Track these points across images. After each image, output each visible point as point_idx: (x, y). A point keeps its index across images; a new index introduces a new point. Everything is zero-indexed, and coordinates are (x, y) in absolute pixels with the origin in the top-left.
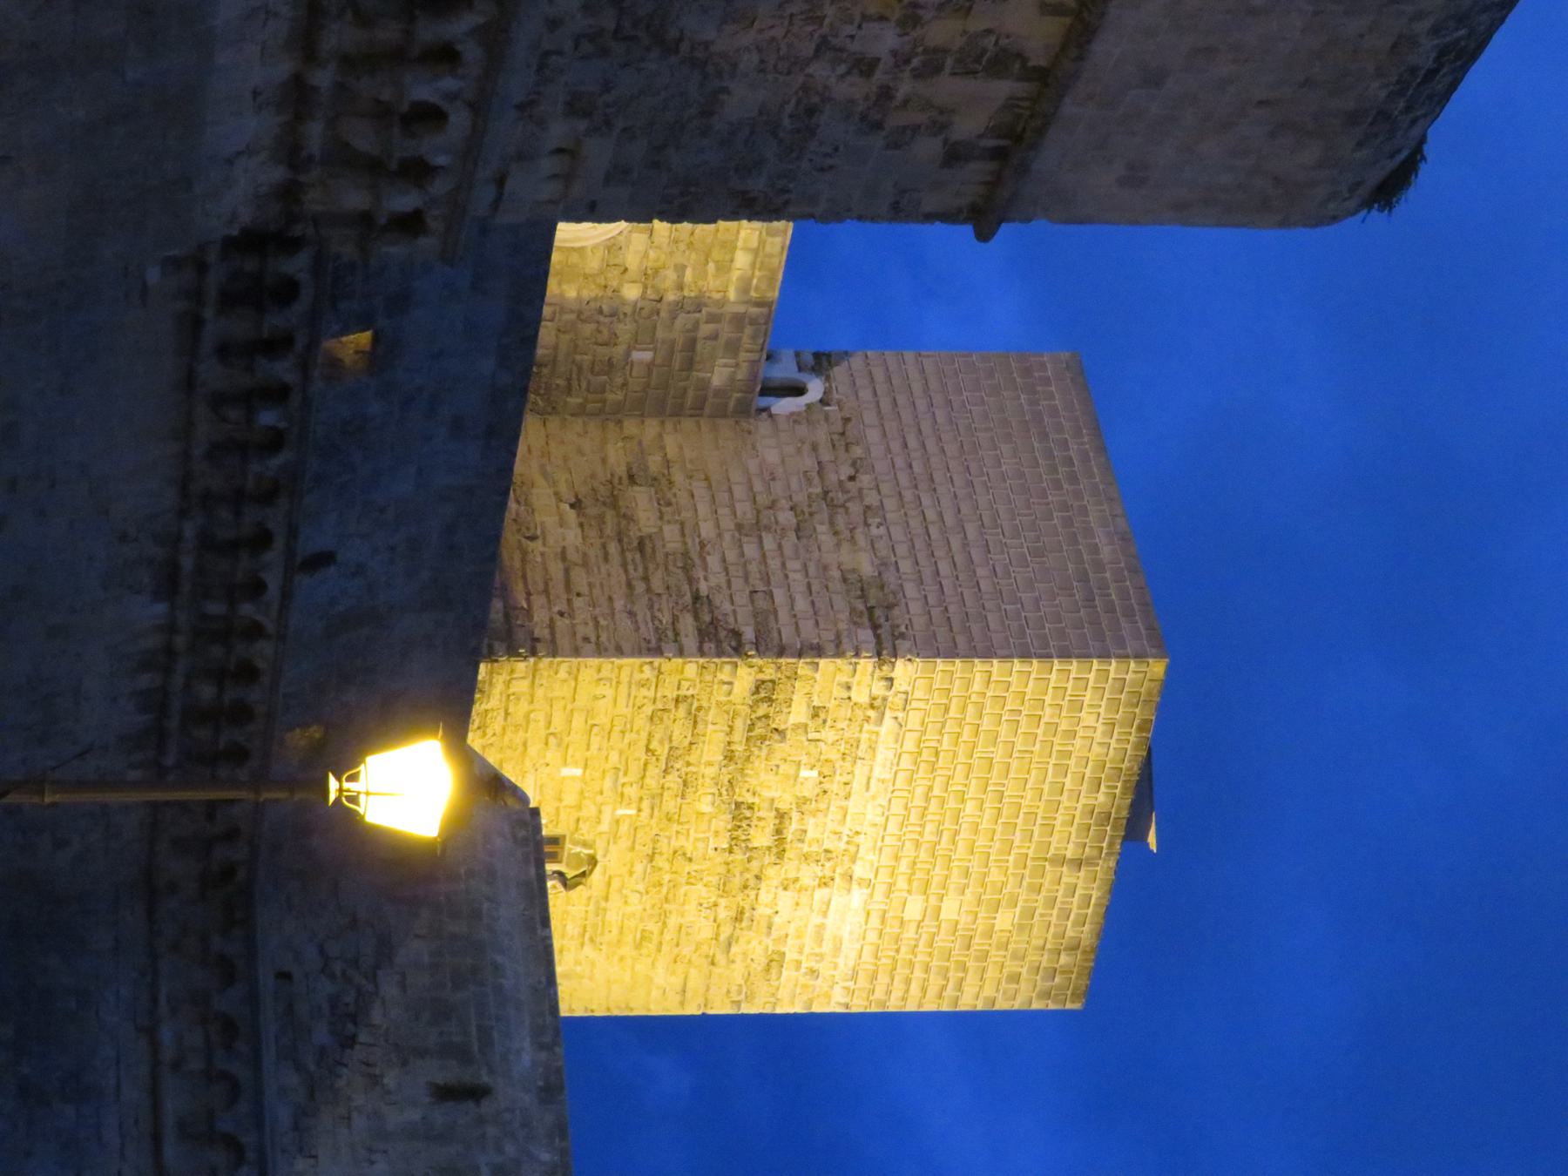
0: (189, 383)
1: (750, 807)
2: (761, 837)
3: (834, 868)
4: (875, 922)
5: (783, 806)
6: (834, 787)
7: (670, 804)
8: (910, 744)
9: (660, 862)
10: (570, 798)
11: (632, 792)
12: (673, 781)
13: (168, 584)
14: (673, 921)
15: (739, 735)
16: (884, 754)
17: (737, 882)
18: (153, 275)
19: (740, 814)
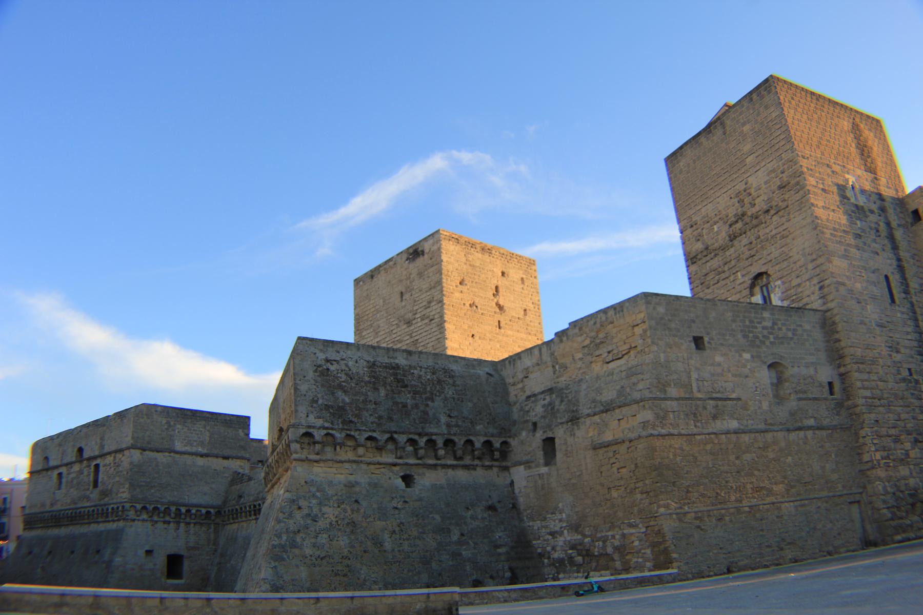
1: (730, 237)
2: (739, 225)
5: (728, 227)
6: (716, 219)
9: (753, 253)
11: (732, 278)
12: (726, 268)
14: (774, 232)
15: (708, 258)
17: (755, 222)
19: (733, 238)
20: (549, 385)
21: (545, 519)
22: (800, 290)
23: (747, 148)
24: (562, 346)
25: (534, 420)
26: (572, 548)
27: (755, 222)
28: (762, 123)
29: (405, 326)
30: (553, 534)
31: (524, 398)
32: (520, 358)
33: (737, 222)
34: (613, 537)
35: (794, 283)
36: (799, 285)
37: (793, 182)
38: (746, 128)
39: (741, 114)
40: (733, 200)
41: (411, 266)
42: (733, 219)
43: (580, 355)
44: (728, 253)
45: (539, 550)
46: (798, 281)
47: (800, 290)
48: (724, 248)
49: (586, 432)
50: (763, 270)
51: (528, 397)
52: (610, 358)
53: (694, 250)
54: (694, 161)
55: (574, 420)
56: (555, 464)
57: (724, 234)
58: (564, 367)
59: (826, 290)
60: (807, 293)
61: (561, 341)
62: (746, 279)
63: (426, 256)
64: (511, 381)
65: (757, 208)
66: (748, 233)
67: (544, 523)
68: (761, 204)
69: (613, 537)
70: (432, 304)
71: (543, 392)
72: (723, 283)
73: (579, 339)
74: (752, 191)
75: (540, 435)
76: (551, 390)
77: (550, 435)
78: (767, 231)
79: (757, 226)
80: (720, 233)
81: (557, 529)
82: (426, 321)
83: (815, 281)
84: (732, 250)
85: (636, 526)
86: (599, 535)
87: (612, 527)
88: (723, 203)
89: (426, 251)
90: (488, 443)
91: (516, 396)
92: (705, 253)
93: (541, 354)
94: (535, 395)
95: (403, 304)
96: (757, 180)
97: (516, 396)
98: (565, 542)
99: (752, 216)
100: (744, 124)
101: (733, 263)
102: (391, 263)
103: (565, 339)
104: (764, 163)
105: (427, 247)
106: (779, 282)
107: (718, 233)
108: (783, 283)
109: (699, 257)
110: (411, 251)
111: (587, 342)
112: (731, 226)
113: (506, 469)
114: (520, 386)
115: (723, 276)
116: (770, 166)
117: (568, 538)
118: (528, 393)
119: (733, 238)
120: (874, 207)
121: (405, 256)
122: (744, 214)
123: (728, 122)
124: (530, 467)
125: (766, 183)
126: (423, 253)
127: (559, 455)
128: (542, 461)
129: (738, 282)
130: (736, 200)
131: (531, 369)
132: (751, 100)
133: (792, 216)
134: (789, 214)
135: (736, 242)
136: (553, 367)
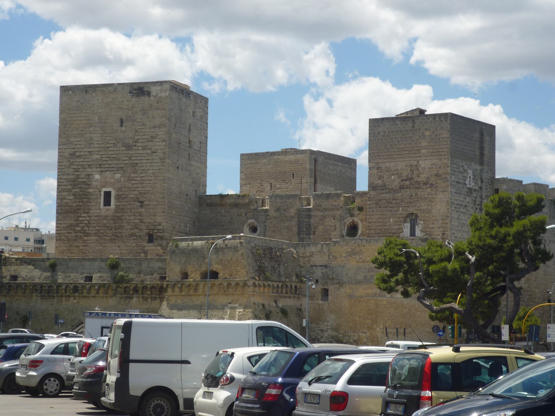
0: (94, 297)
1: (400, 186)
2: (407, 183)
3: (415, 168)
4: (427, 158)
5: (400, 180)
6: (395, 173)
7: (398, 201)
8: (386, 161)
9: (411, 201)
10: (397, 220)
11: (396, 209)
12: (394, 202)
13: (131, 298)
14: (426, 196)
15: (384, 192)
16: (388, 164)
17: (416, 185)
18: (75, 301)
19: (402, 188)
20: (325, 263)
21: (318, 324)
22: (432, 230)
23: (424, 144)
24: (335, 248)
25: (317, 278)
26: (332, 338)
27: (416, 185)
28: (436, 135)
29: (124, 148)
30: (322, 331)
31: (309, 265)
32: (309, 246)
33: (406, 180)
34: (354, 336)
35: (431, 226)
36: (432, 228)
37: (444, 176)
38: (427, 133)
39: (426, 122)
40: (407, 168)
41: (134, 99)
42: (404, 178)
43: (345, 255)
44: (397, 195)
45: (313, 337)
46: (433, 226)
47: (432, 230)
48: (395, 191)
49: (346, 290)
50: (415, 212)
51: (312, 266)
52: (361, 260)
53: (376, 182)
54: (389, 132)
55: (341, 284)
56: (327, 300)
57: (397, 183)
58: (335, 258)
59: (445, 236)
60: (436, 234)
61: (335, 245)
62: (404, 213)
63: (152, 98)
64: (302, 255)
65: (420, 180)
66: (412, 190)
67: (317, 325)
68: (423, 178)
69: (354, 336)
70: (155, 140)
71: (321, 266)
72: (390, 209)
73: (346, 248)
74: (420, 169)
75: (320, 287)
76: (326, 266)
77: (326, 287)
78: (423, 193)
79: (417, 188)
80: (395, 182)
81: (325, 329)
82: (149, 152)
83: (441, 229)
84: (400, 194)
85: (365, 333)
86: (347, 334)
87: (354, 332)
88: (401, 165)
89: (153, 93)
90: (296, 286)
91: (304, 263)
92: (382, 188)
93: (322, 247)
94: (316, 266)
95: (123, 129)
96: (425, 164)
97: (304, 263)
98: (328, 335)
99: (416, 182)
100: (426, 130)
101: (398, 201)
102: (110, 88)
103: (337, 245)
104: (431, 158)
105: (154, 90)
106: (422, 222)
107: (394, 181)
108: (424, 223)
109: (378, 188)
110: (136, 87)
111: (350, 250)
112: (402, 181)
113: (298, 298)
114: (308, 259)
115: (391, 205)
116: (434, 161)
117: (331, 334)
118: (312, 263)
119: (402, 188)
120: (477, 188)
121: (128, 89)
122: (412, 179)
123: (417, 123)
124: (312, 299)
125: (429, 168)
126: (149, 94)
127: (330, 297)
128: (320, 298)
129: (399, 212)
130: (409, 168)
131: (315, 253)
132: (435, 119)
133: (438, 193)
134: (437, 191)
135: (403, 191)
136: (329, 256)
